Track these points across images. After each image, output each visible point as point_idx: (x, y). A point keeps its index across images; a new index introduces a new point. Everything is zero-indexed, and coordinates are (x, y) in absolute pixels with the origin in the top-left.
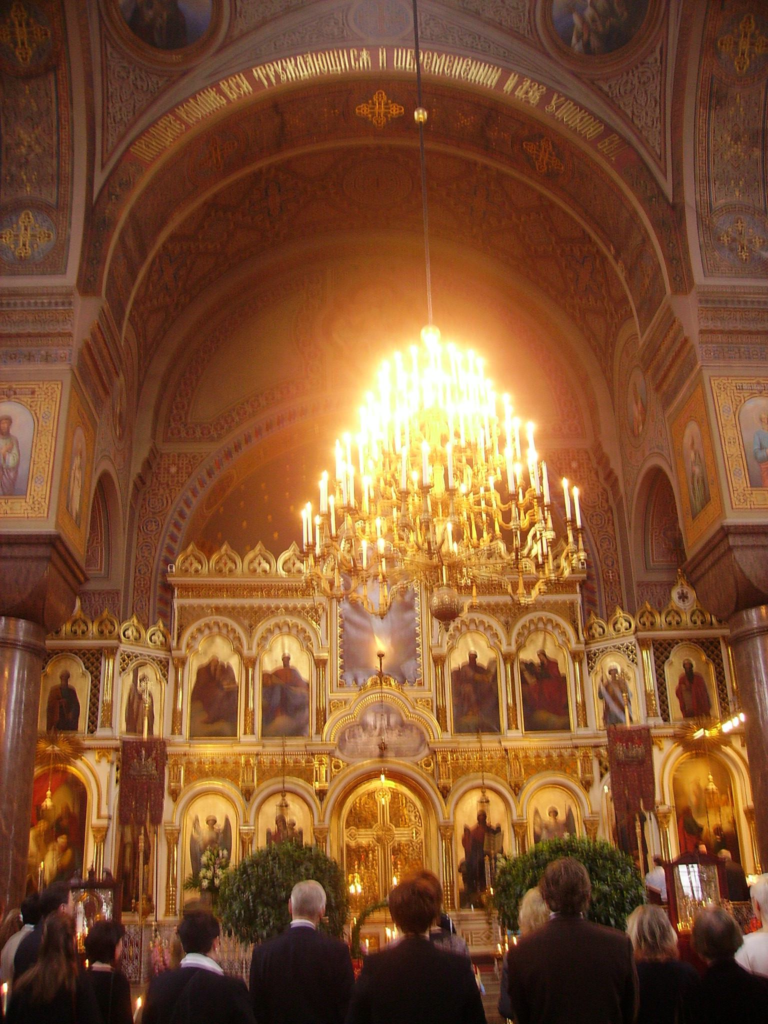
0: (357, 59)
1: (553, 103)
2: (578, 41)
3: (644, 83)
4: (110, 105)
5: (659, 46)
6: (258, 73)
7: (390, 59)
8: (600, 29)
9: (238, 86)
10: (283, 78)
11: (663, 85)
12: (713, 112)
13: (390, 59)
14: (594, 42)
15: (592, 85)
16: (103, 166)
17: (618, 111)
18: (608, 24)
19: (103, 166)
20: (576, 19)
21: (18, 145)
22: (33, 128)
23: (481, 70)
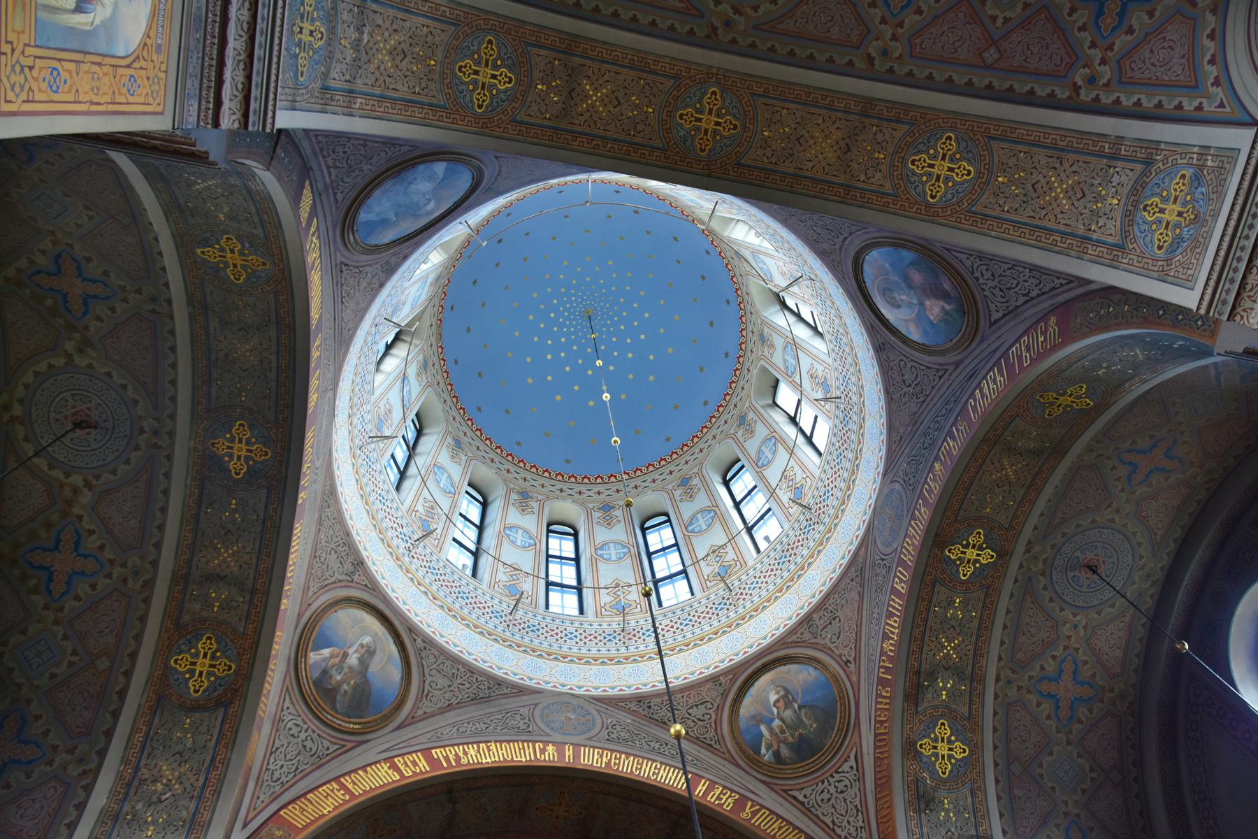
0: (543, 751)
1: (747, 810)
2: (768, 750)
3: (842, 792)
4: (272, 760)
5: (852, 755)
6: (437, 753)
7: (576, 755)
8: (791, 740)
9: (415, 764)
10: (465, 761)
11: (863, 791)
12: (923, 815)
13: (576, 755)
14: (785, 752)
15: (786, 794)
16: (245, 825)
17: (817, 820)
18: (797, 734)
19: (245, 825)
20: (763, 728)
21: (155, 781)
22: (180, 765)
23: (670, 774)
